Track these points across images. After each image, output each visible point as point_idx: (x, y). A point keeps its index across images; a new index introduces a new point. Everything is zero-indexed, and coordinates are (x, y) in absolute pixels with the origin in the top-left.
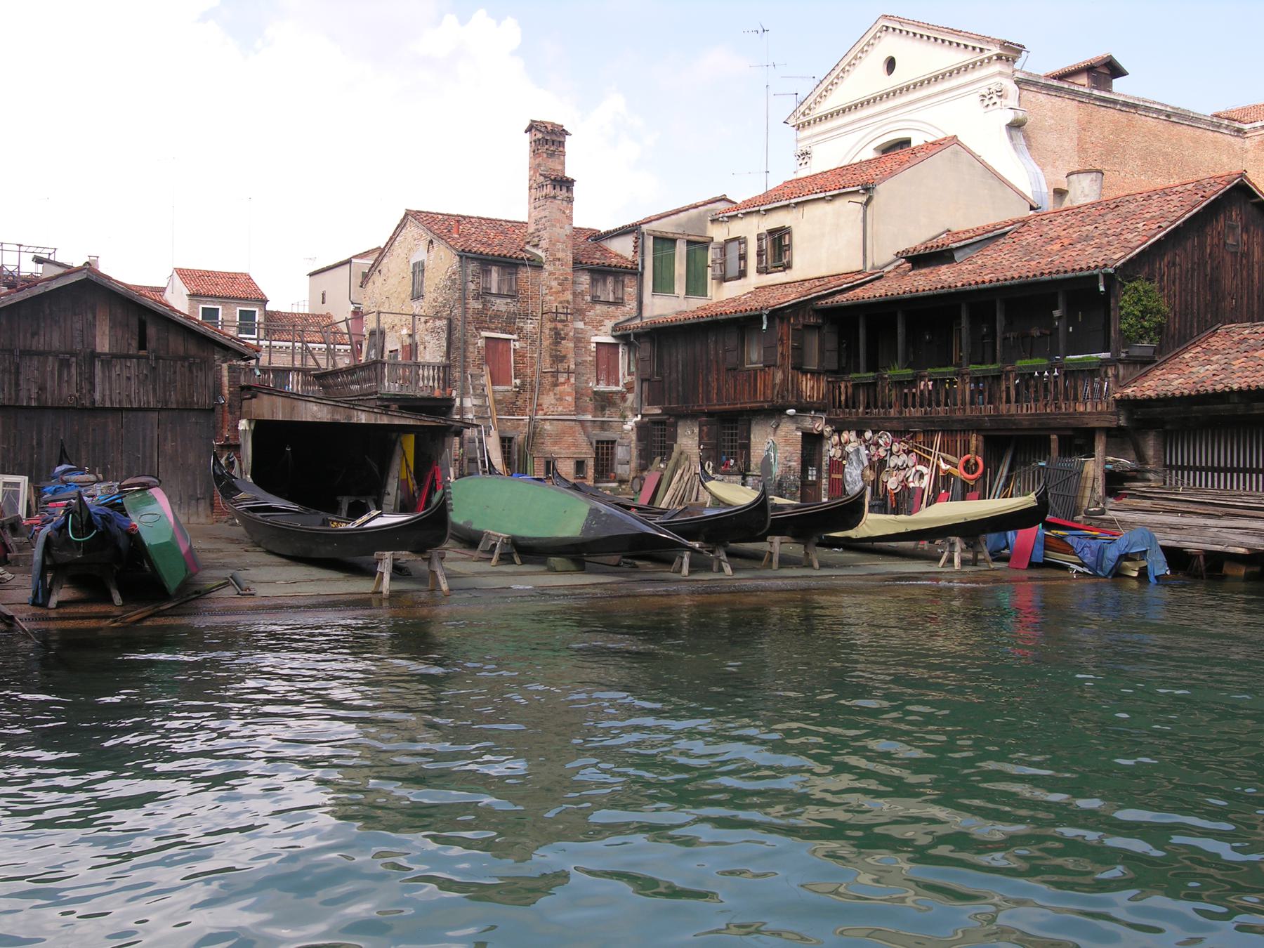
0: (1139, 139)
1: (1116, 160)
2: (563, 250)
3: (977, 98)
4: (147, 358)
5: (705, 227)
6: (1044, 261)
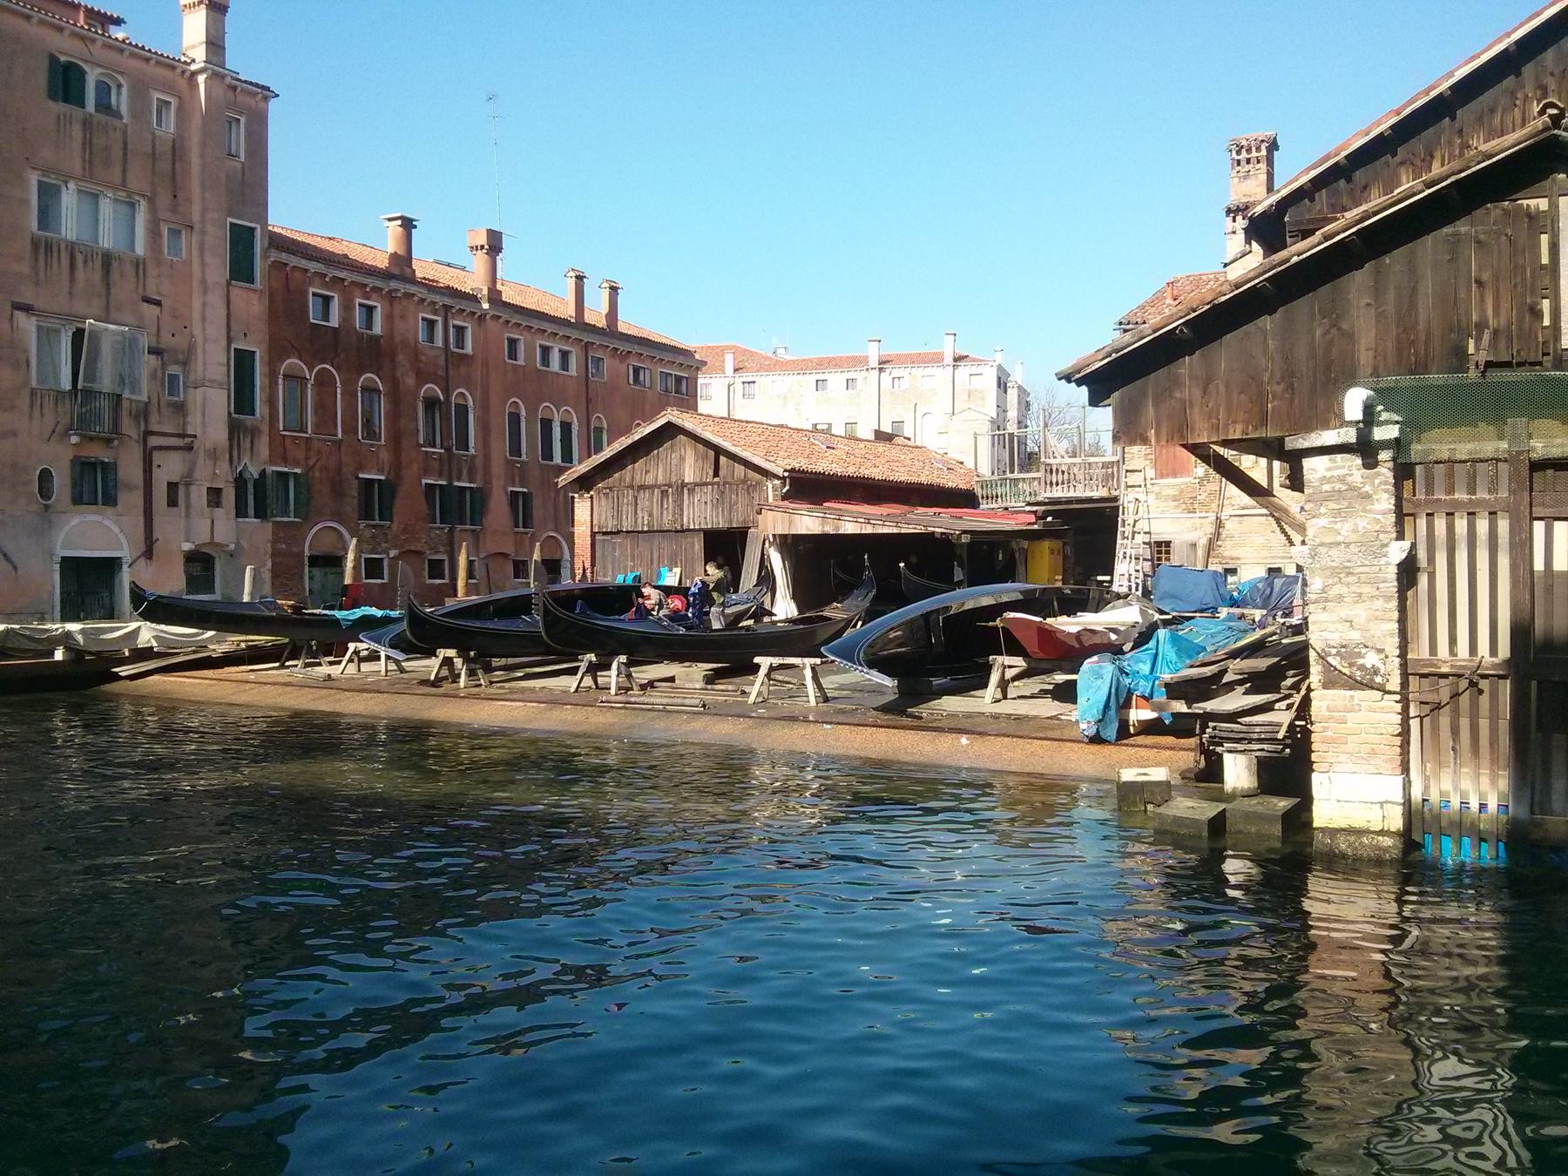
4: (718, 483)
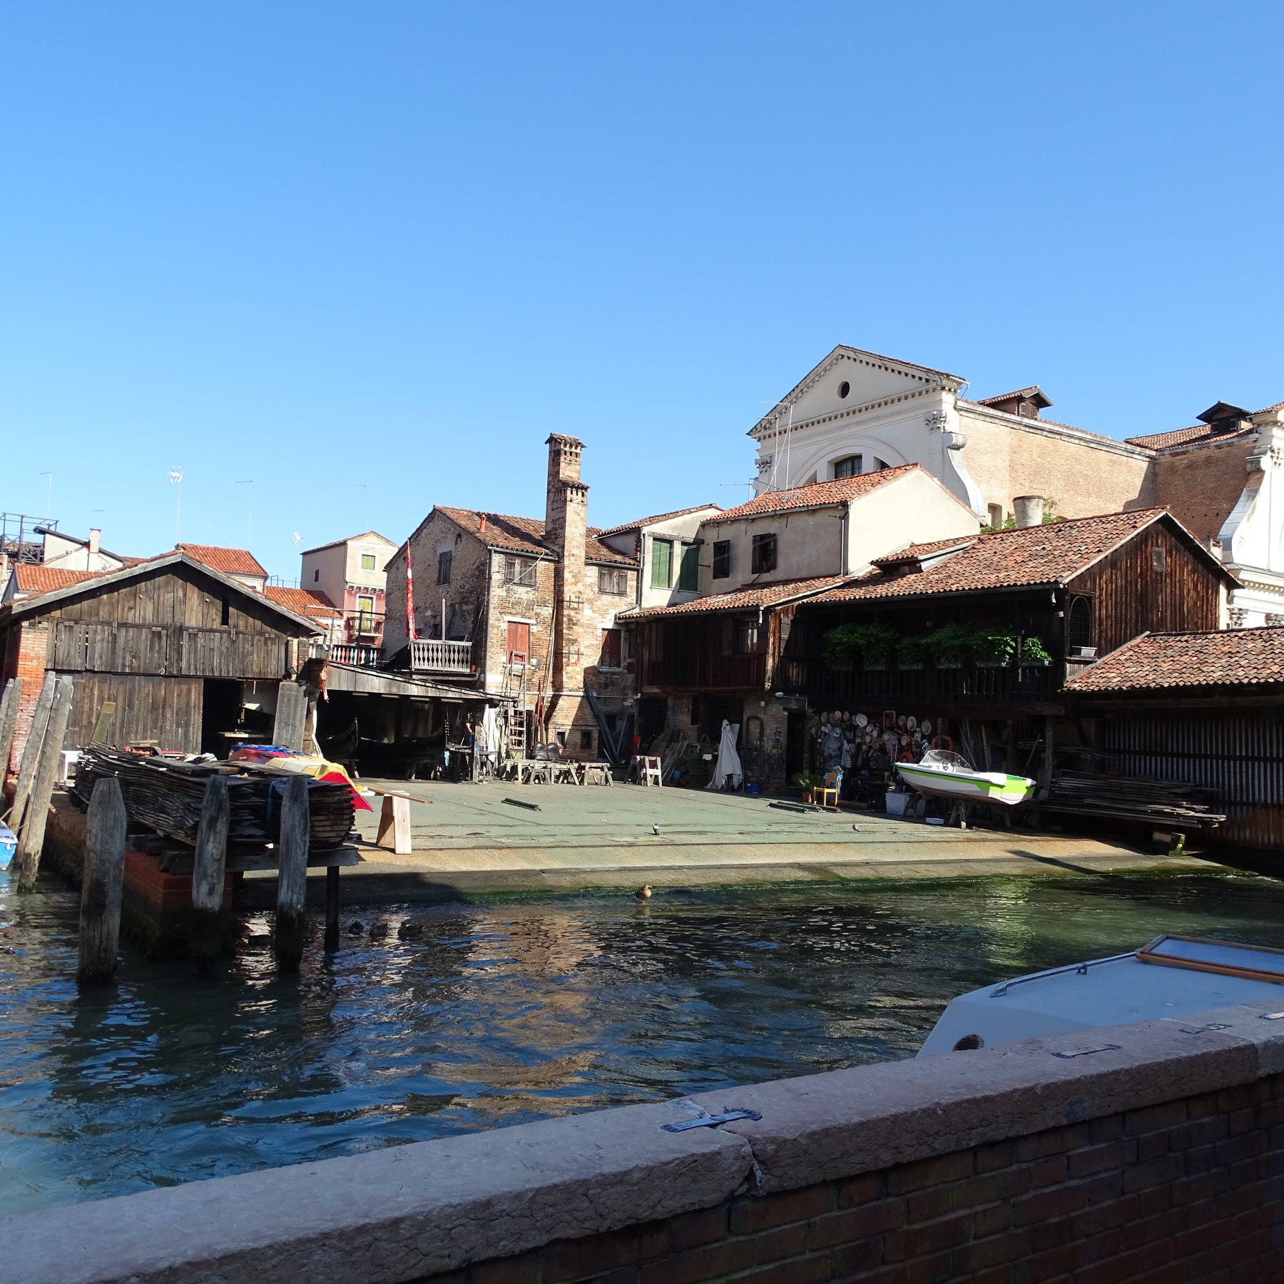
2: (577, 547)
3: (922, 422)
6: (1001, 575)
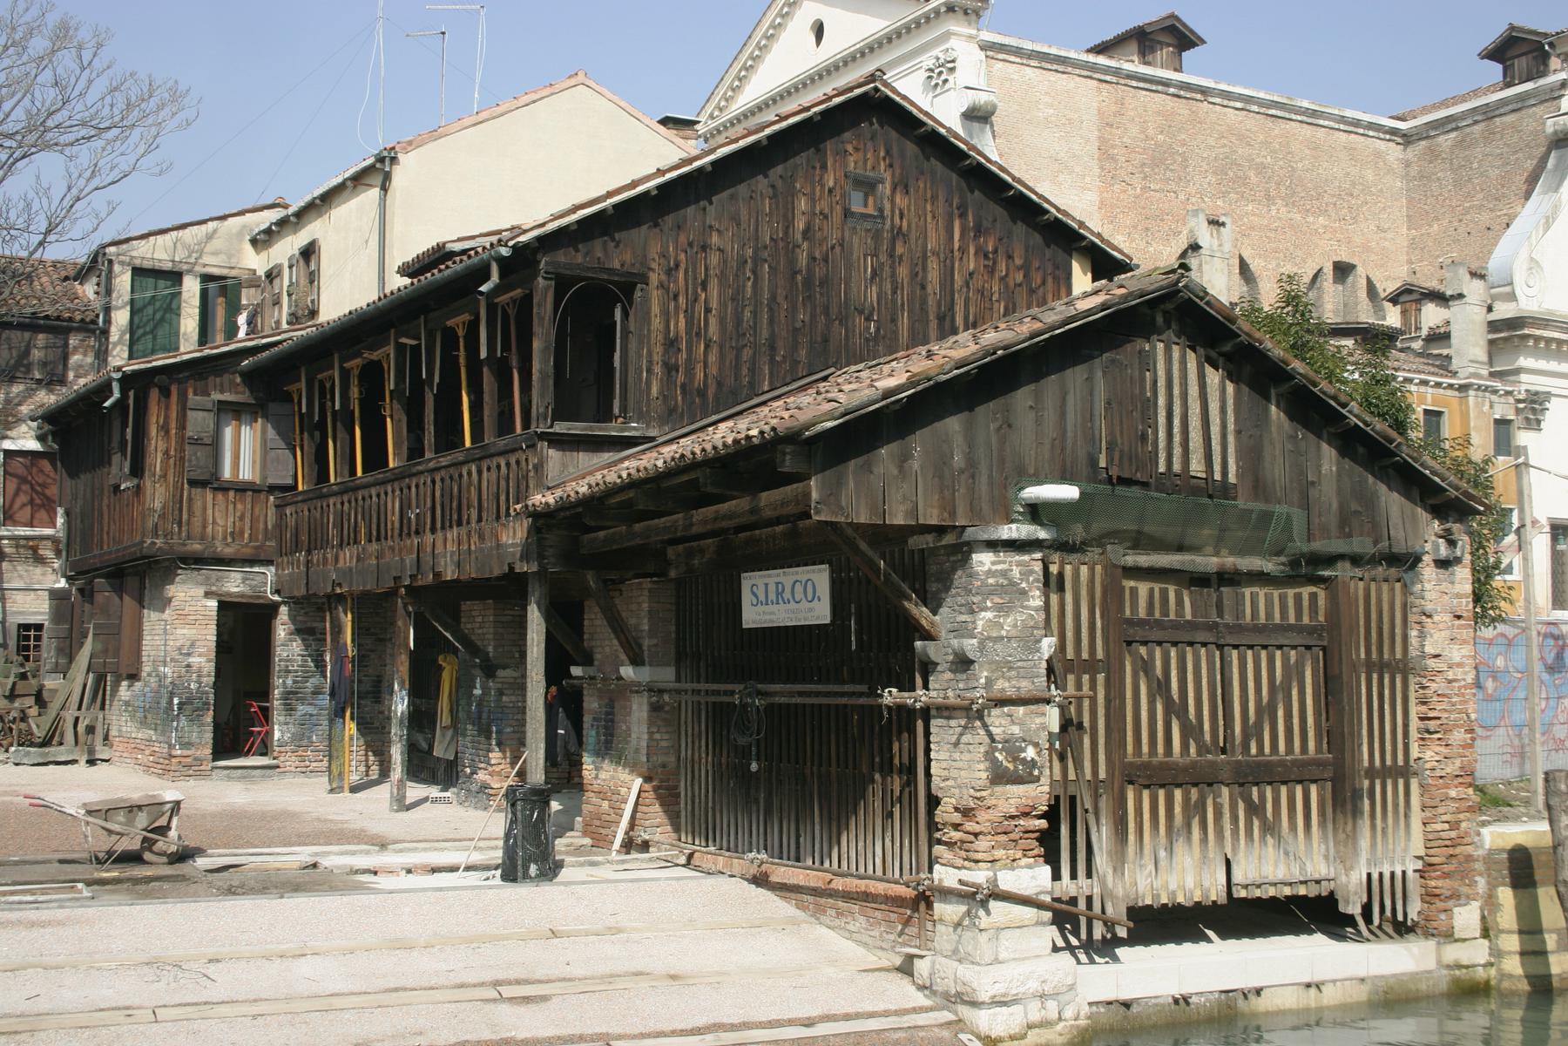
0: (1211, 142)
1: (1169, 173)
5: (240, 251)
